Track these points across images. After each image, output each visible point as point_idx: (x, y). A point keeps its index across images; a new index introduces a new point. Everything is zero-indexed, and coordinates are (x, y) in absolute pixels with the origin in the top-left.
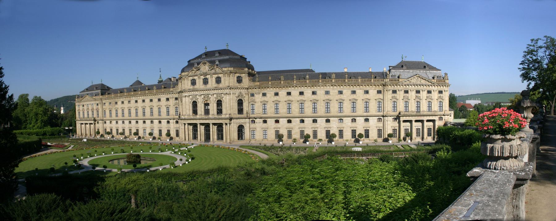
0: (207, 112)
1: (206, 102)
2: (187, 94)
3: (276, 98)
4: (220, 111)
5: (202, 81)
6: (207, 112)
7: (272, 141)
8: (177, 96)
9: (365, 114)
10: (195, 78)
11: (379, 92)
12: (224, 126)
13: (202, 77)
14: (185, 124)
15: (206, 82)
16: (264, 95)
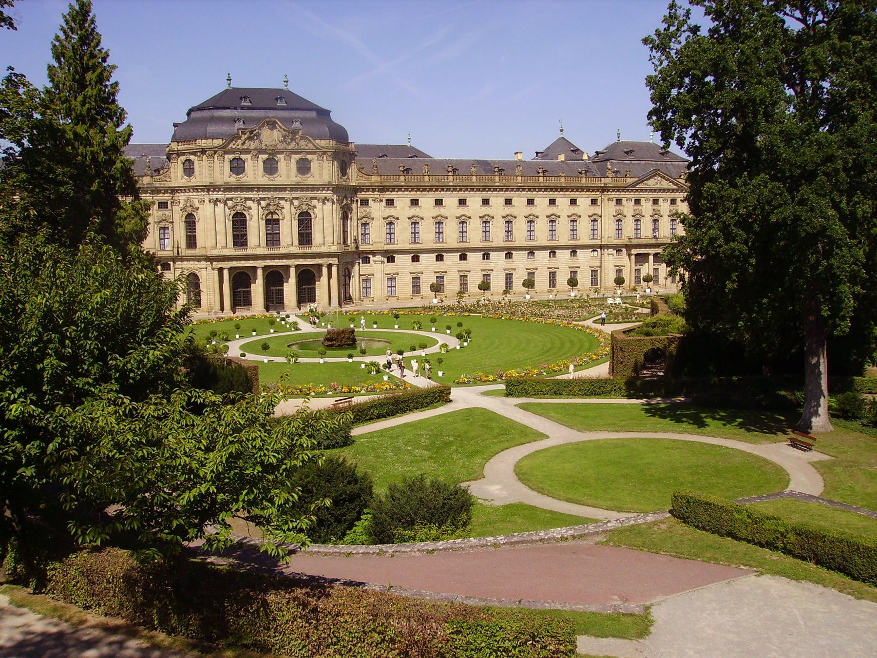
0: (273, 239)
1: (269, 217)
2: (220, 195)
3: (414, 211)
4: (305, 238)
5: (261, 164)
6: (273, 239)
7: (406, 299)
8: (165, 197)
9: (572, 243)
10: (243, 157)
11: (594, 202)
12: (325, 270)
13: (265, 156)
14: (221, 270)
15: (270, 167)
16: (390, 203)
